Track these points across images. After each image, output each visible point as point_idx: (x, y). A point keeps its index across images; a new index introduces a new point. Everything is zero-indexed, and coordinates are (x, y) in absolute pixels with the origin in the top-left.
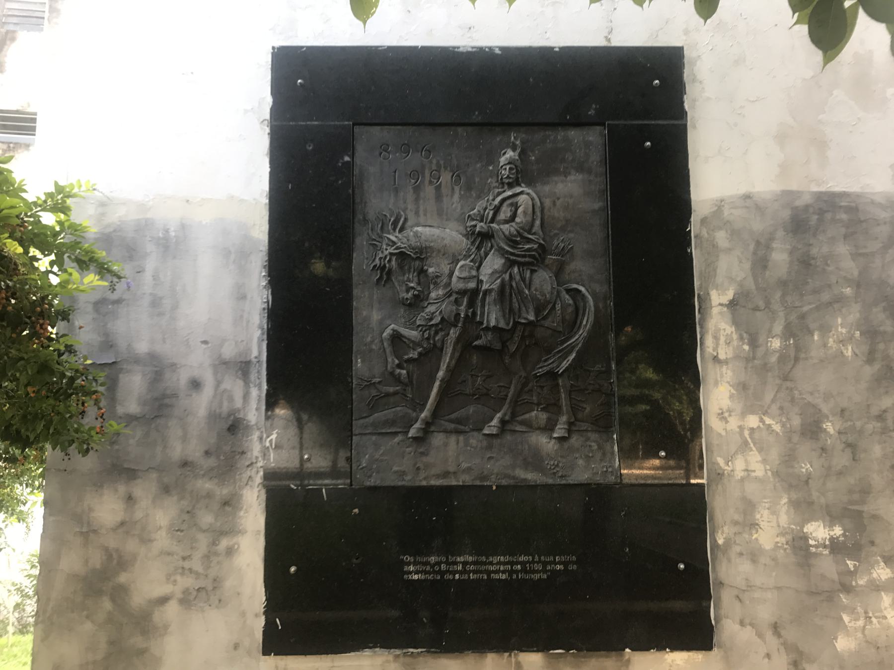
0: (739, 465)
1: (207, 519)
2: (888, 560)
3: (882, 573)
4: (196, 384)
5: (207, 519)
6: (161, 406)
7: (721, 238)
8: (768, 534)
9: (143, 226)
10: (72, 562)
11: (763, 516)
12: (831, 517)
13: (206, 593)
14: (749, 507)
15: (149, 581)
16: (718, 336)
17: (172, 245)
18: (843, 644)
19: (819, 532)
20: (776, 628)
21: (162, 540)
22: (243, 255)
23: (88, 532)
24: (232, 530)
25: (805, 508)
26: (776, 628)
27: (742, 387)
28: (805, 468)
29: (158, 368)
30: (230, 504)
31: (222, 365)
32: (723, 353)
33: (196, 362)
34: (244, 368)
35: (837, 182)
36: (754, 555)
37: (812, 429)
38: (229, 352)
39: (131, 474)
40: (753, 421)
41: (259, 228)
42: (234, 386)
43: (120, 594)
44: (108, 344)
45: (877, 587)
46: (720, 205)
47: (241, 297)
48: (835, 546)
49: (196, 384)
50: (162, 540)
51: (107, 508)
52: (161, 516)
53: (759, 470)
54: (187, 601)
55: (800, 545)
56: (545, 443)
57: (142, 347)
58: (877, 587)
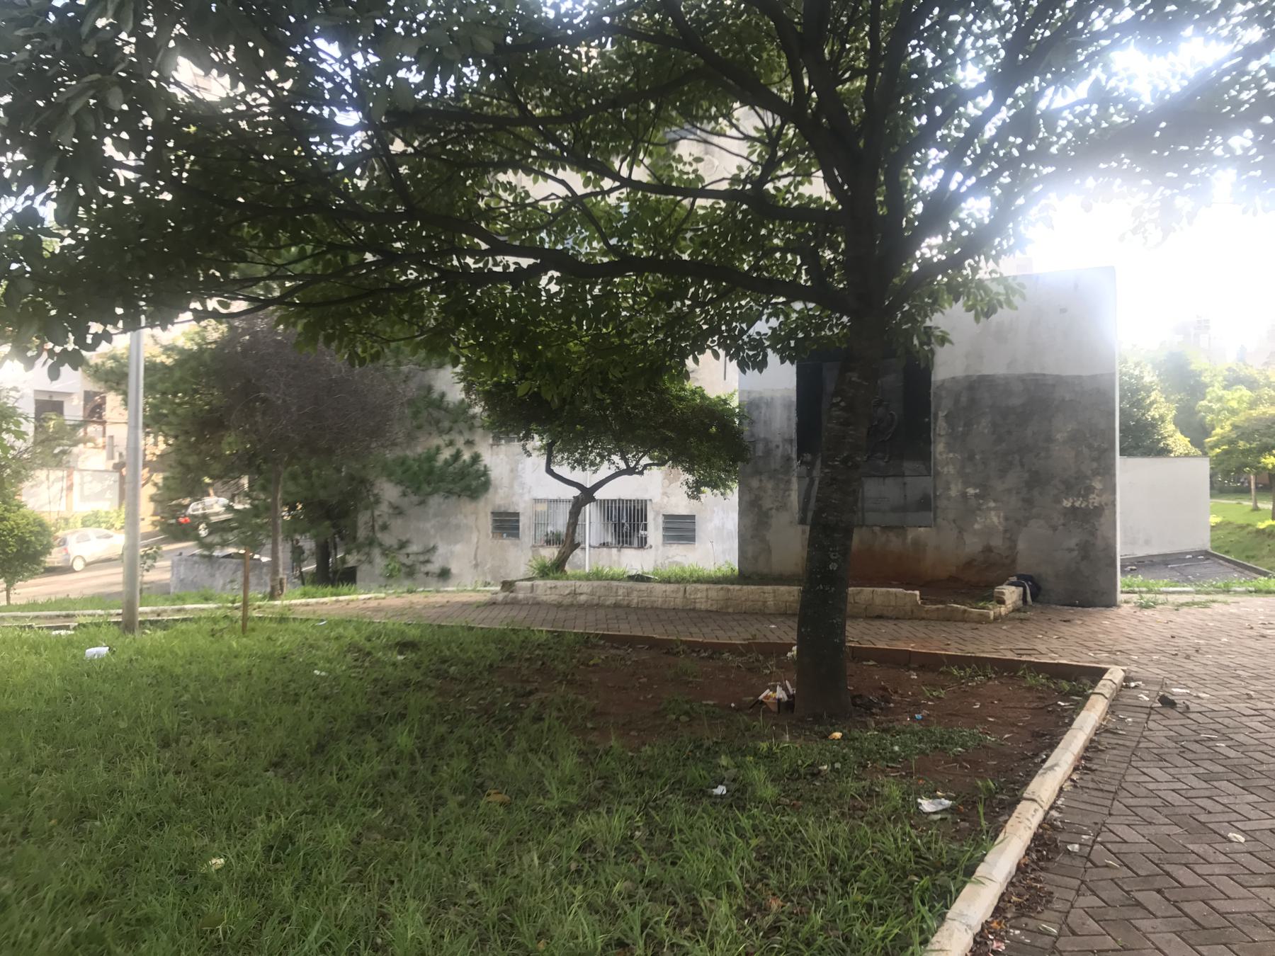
0: (946, 469)
1: (782, 486)
2: (995, 501)
3: (992, 504)
4: (777, 447)
5: (782, 486)
6: (768, 453)
7: (944, 393)
8: (954, 492)
9: (761, 398)
10: (747, 498)
11: (953, 486)
12: (975, 486)
13: (783, 507)
14: (948, 483)
15: (767, 503)
16: (941, 427)
17: (769, 404)
18: (977, 526)
19: (971, 491)
20: (954, 521)
21: (770, 492)
22: (789, 406)
23: (750, 490)
24: (789, 489)
25: (967, 484)
26: (954, 521)
27: (947, 444)
28: (968, 470)
29: (767, 442)
30: (789, 482)
31: (785, 440)
32: (943, 433)
33: (778, 440)
34: (791, 441)
35: (987, 370)
36: (949, 498)
37: (971, 458)
38: (786, 436)
39: (761, 473)
40: (951, 455)
41: (794, 399)
42: (788, 447)
43: (760, 507)
44: (752, 435)
45: (990, 509)
46: (943, 381)
47: (789, 419)
48: (976, 495)
49: (777, 447)
50: (770, 492)
51: (755, 483)
52: (769, 485)
53: (952, 471)
54: (777, 509)
55: (964, 495)
56: (882, 463)
57: (762, 436)
58: (990, 509)
